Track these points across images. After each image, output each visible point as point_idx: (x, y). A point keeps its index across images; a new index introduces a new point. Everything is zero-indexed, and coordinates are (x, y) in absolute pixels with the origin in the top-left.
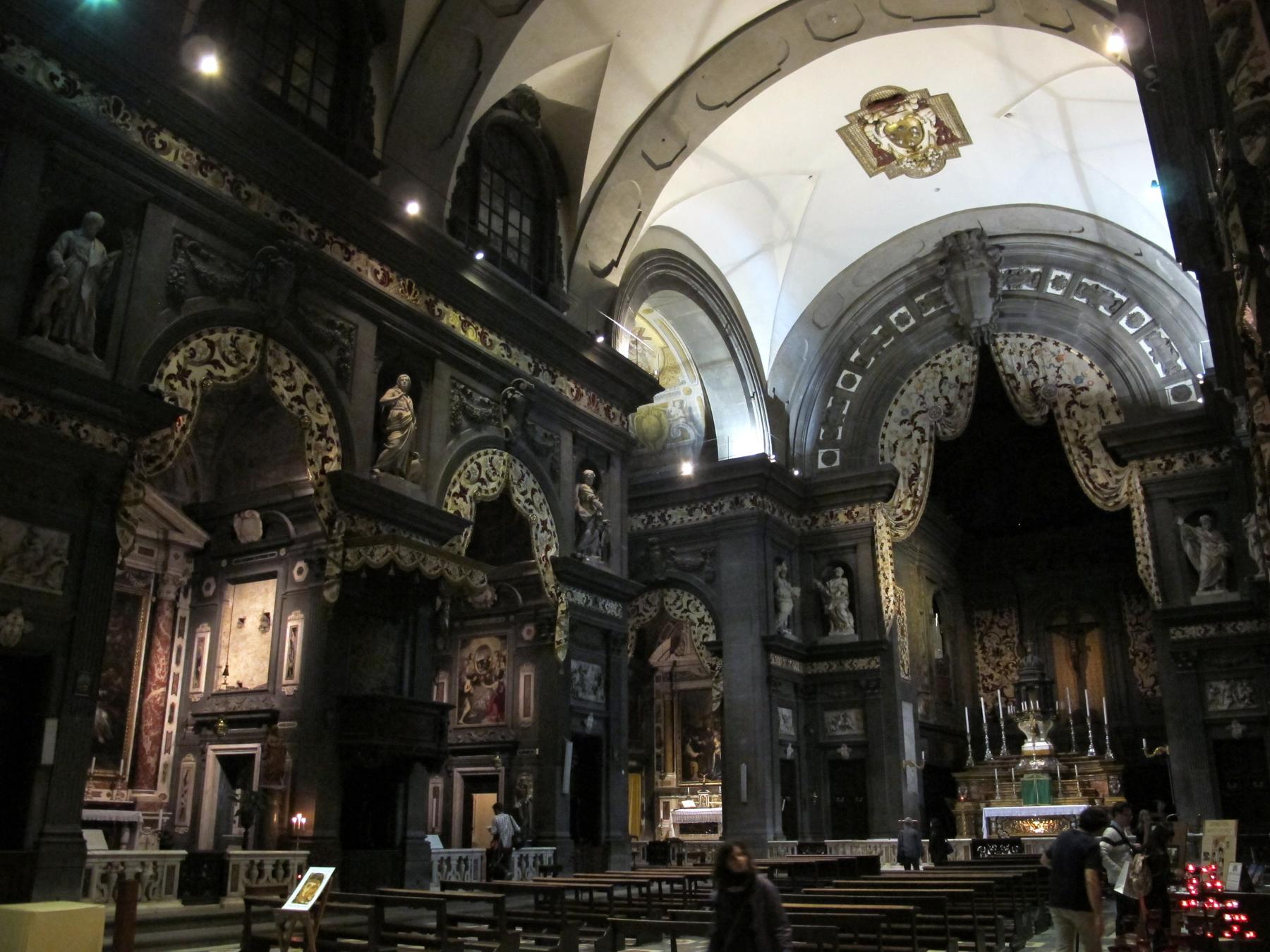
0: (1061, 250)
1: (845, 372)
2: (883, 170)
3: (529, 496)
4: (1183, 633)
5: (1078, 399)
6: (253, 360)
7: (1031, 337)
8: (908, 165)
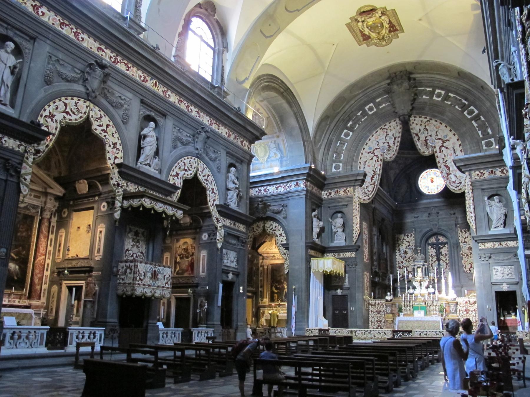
0: (440, 81)
1: (346, 131)
3: (206, 177)
4: (485, 246)
5: (445, 145)
6: (85, 113)
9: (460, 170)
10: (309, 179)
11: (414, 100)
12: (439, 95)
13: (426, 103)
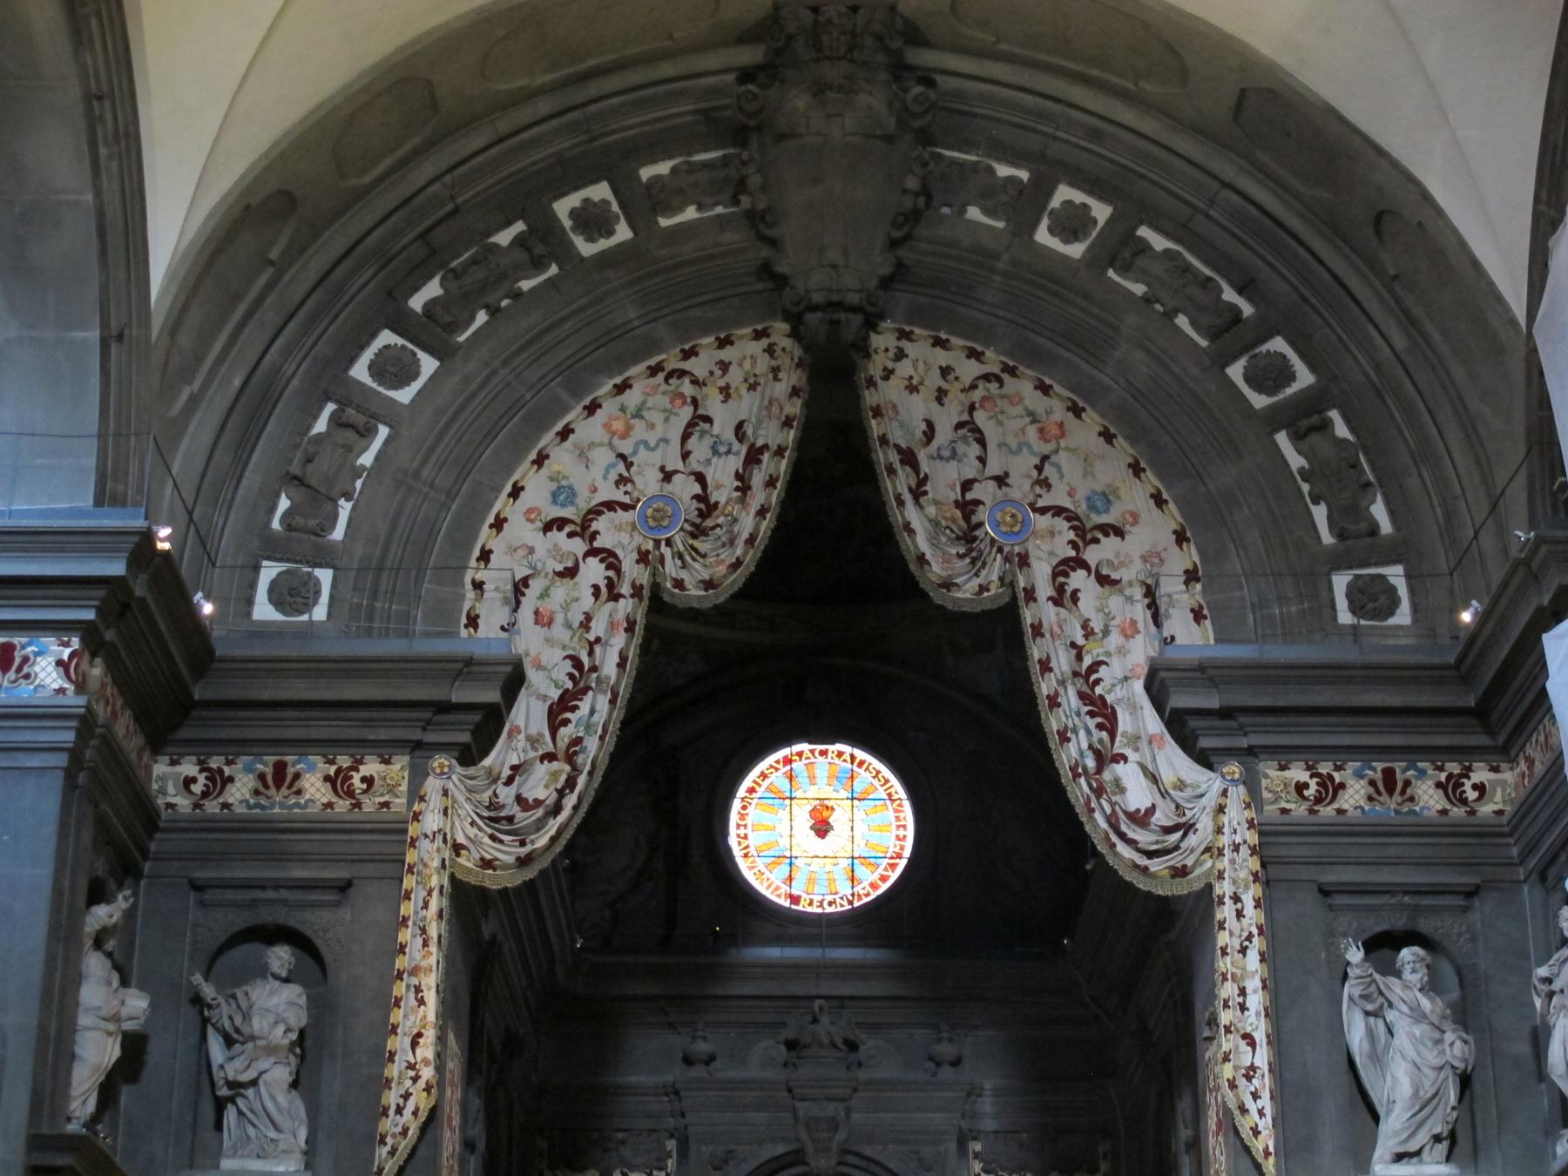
0: (1096, 135)
1: (387, 338)
5: (1092, 555)
7: (973, 354)
9: (1186, 742)
10: (110, 635)
11: (914, 216)
12: (1072, 224)
13: (996, 257)
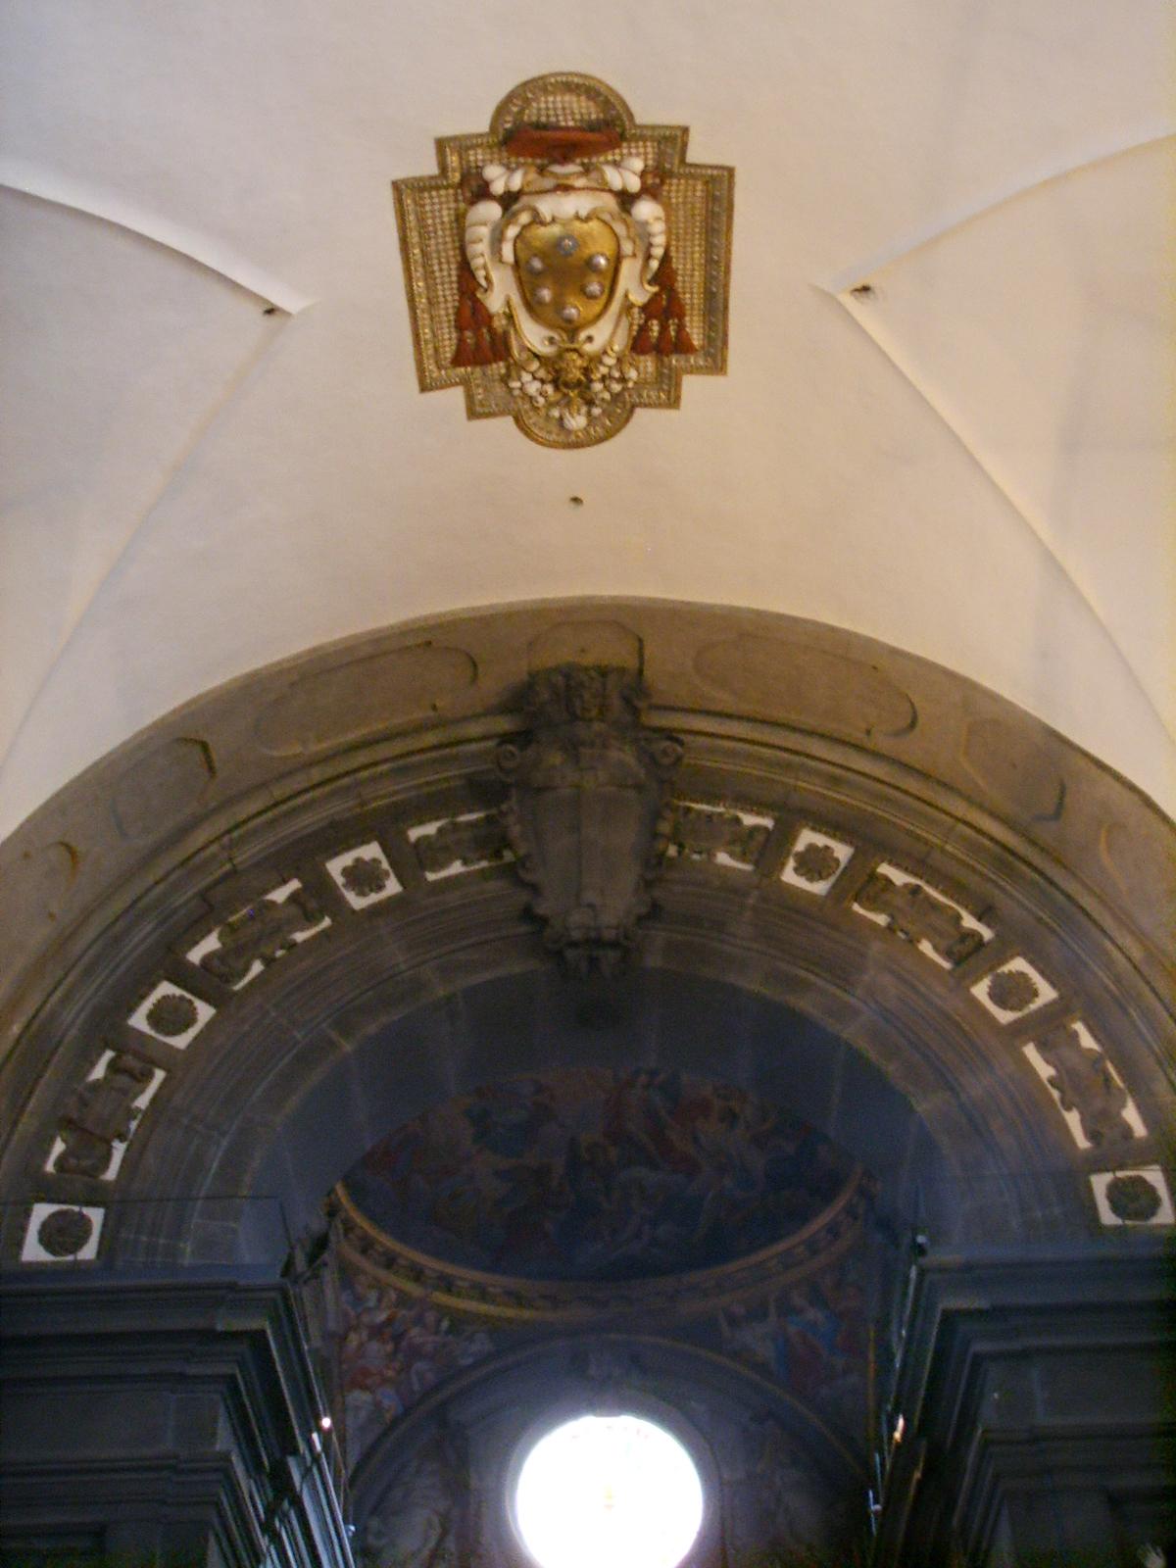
0: (835, 781)
1: (166, 989)
2: (465, 382)
8: (533, 388)
12: (814, 863)
